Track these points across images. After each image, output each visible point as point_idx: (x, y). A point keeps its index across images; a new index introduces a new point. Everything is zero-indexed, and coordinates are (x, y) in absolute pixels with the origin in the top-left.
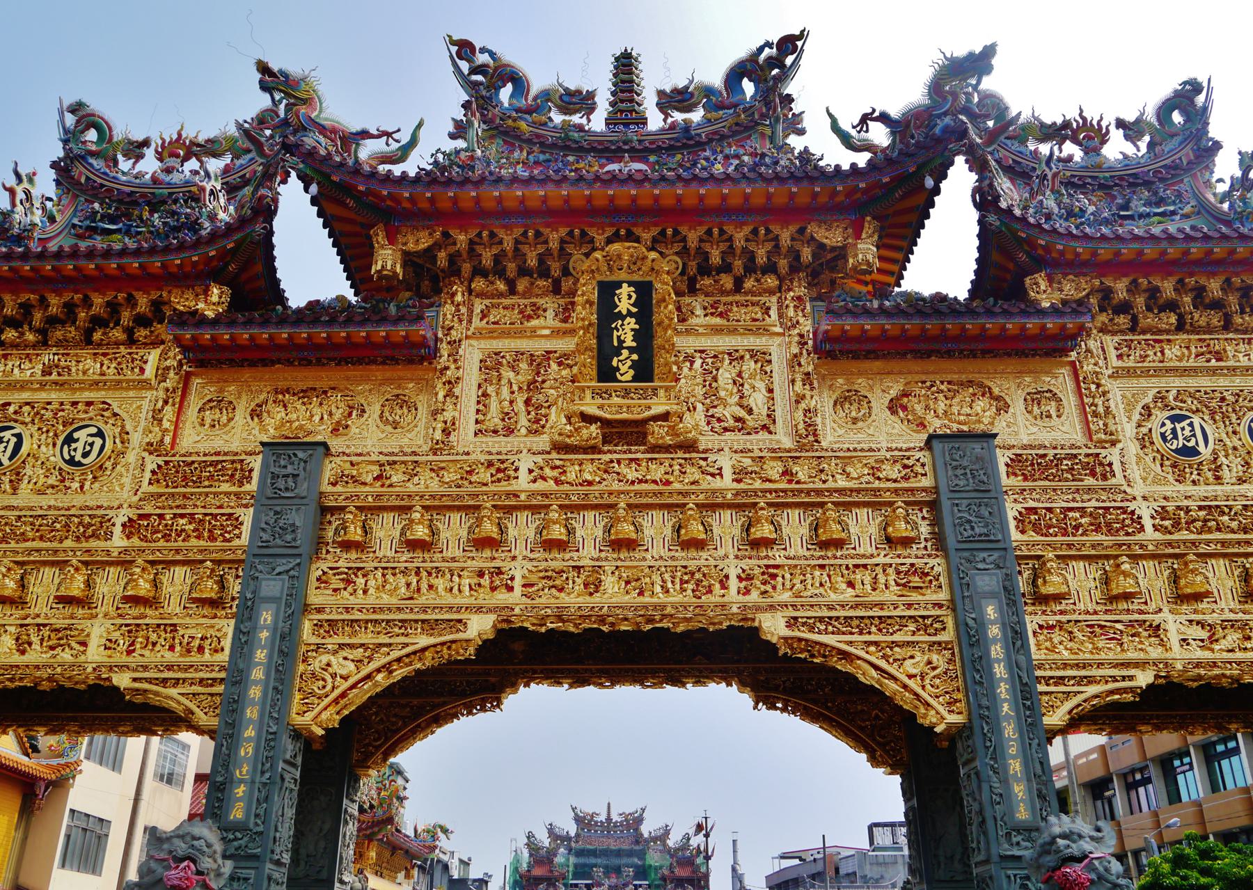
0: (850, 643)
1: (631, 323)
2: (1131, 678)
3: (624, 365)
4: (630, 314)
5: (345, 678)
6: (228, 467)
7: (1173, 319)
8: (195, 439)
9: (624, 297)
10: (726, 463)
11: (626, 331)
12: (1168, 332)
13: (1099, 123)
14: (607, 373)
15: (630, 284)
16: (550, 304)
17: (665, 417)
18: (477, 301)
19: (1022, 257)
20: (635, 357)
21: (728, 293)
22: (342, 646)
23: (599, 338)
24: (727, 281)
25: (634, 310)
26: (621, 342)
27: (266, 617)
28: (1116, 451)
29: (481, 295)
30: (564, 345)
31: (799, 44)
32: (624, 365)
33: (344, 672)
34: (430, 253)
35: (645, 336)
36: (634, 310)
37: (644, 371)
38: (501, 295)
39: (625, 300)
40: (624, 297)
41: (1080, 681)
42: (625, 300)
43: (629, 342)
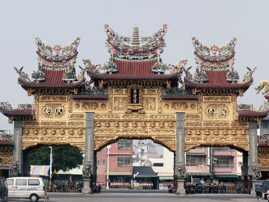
0: (163, 140)
1: (136, 95)
2: (197, 145)
3: (135, 100)
4: (136, 93)
5: (100, 144)
6: (82, 116)
7: (212, 94)
8: (76, 111)
9: (135, 91)
10: (148, 115)
11: (135, 96)
12: (212, 96)
13: (217, 46)
14: (132, 102)
15: (136, 89)
16: (124, 90)
17: (140, 109)
18: (113, 89)
19: (191, 87)
20: (136, 100)
21: (150, 88)
22: (99, 140)
23: (131, 97)
24: (150, 87)
25: (136, 93)
26: (134, 97)
27: (89, 136)
28: (201, 114)
29: (114, 88)
30: (127, 96)
31: (167, 26)
32: (135, 100)
33: (99, 143)
34: (107, 83)
35: (138, 97)
36: (136, 93)
37: (138, 102)
38: (117, 88)
39: (135, 91)
40: (135, 91)
41: (190, 145)
42: (135, 91)
43: (135, 98)
